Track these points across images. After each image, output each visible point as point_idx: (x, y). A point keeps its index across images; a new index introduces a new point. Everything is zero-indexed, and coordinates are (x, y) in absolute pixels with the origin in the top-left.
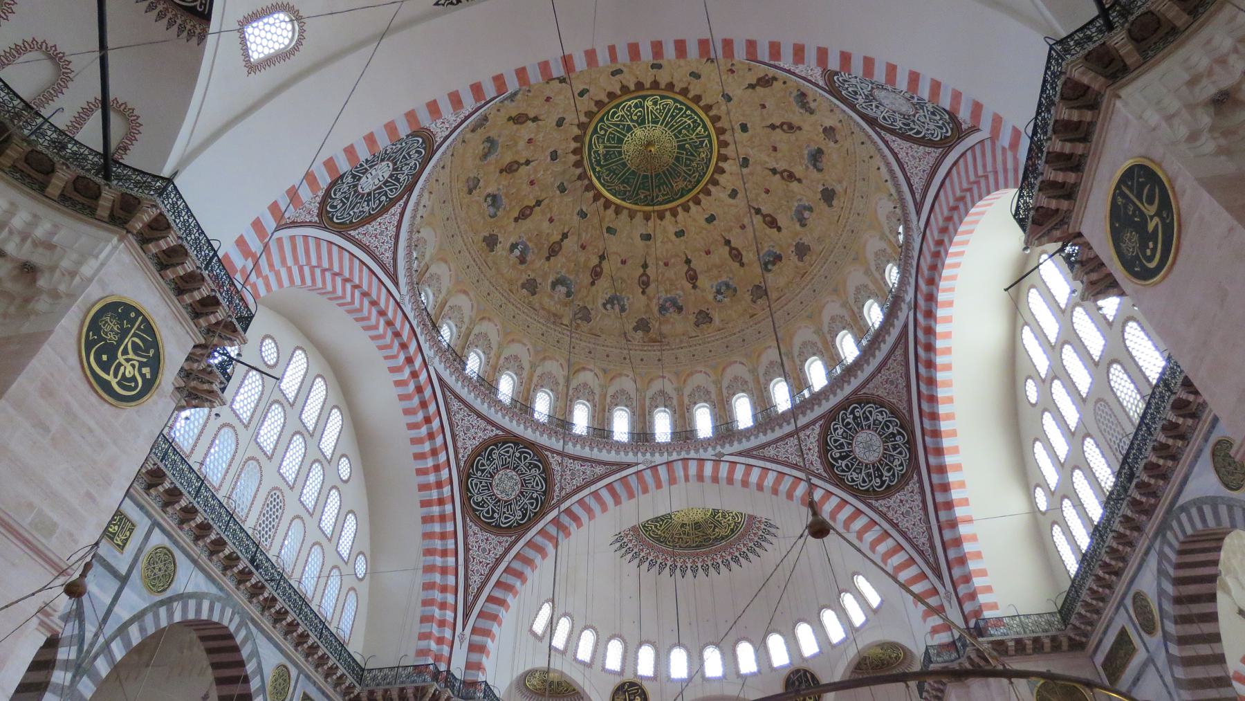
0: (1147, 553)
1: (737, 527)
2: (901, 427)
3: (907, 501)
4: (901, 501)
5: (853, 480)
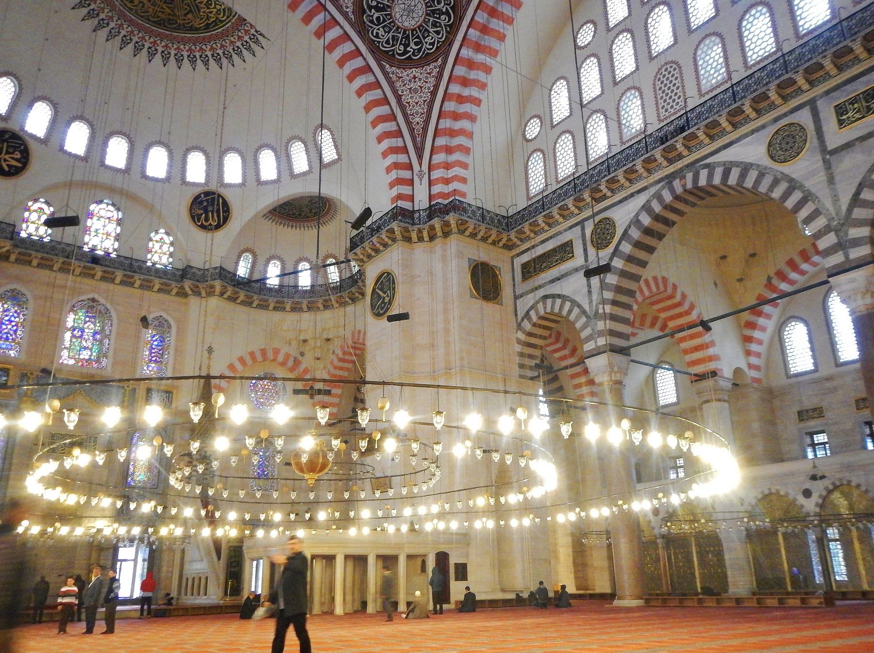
0: (639, 191)
1: (217, 25)
2: (453, 8)
3: (420, 80)
4: (415, 77)
5: (377, 36)
